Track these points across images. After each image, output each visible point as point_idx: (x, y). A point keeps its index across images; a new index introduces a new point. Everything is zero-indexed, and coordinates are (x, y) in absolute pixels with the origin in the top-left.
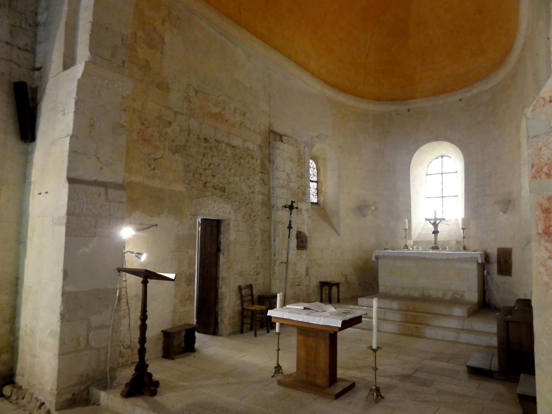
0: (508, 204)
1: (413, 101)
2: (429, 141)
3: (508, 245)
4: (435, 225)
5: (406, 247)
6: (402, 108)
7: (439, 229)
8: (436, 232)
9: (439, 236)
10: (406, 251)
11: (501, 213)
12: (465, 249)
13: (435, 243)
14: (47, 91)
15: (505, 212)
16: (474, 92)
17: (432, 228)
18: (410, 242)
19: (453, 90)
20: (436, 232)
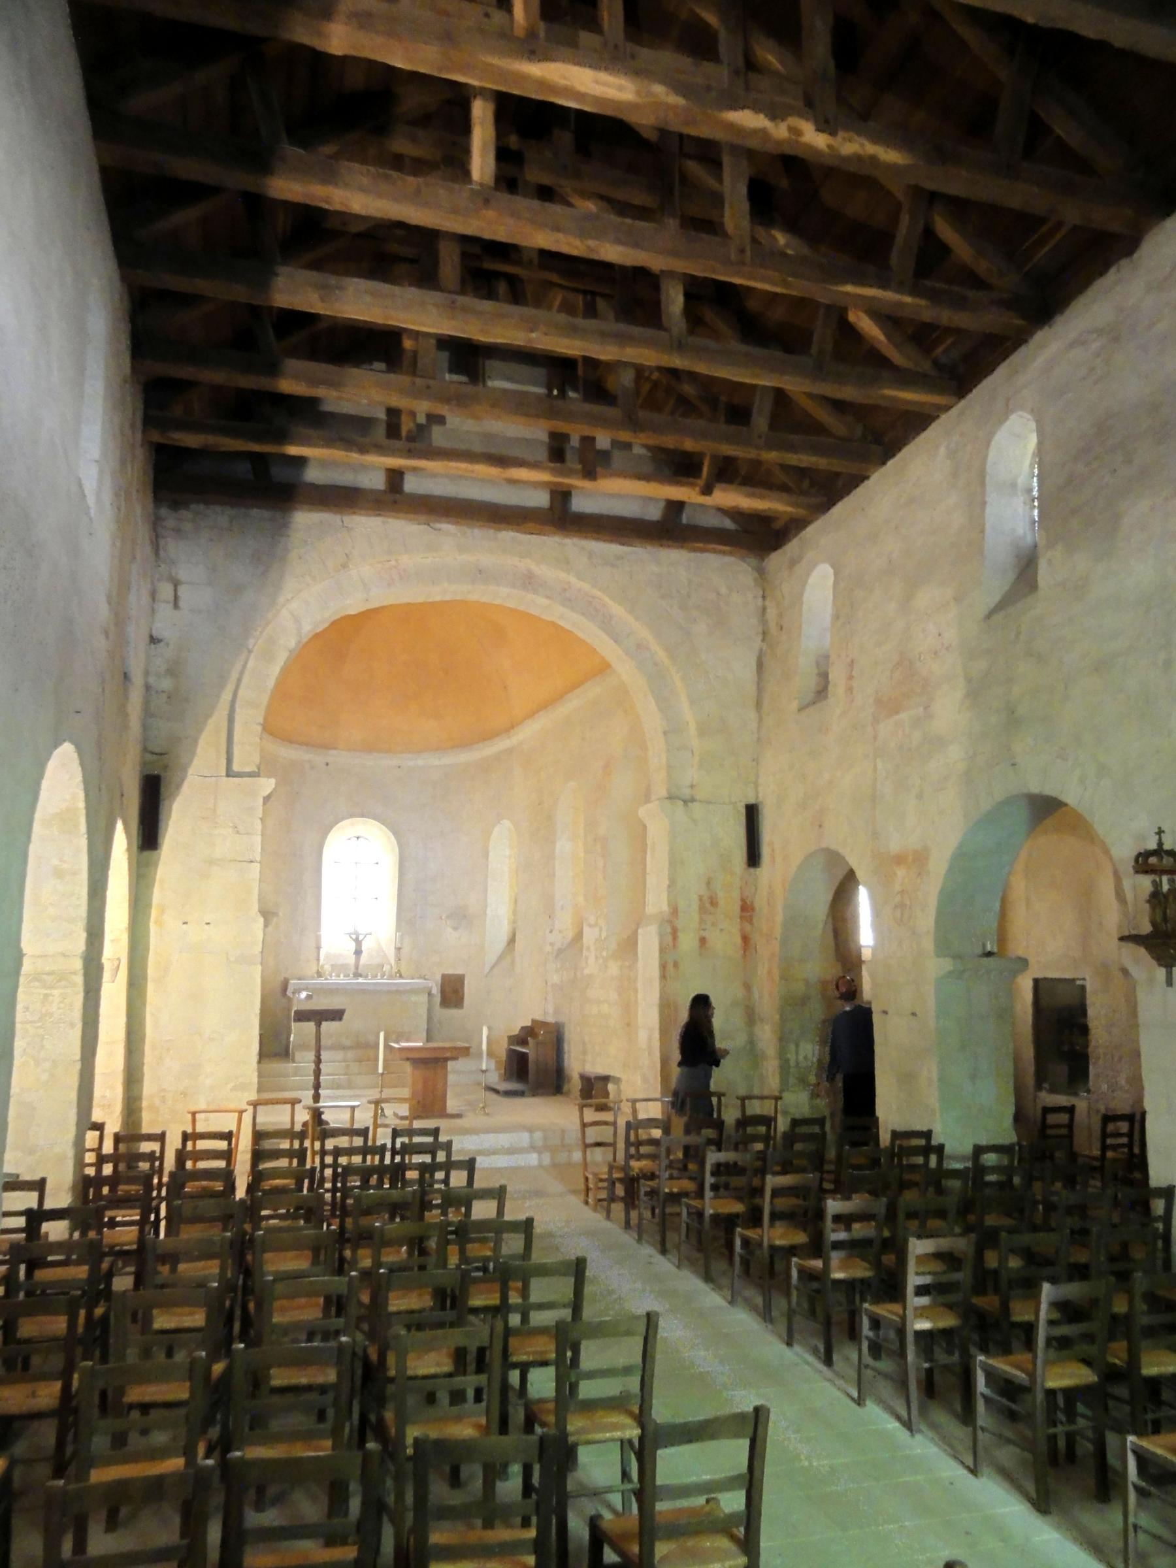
0: (461, 917)
1: (334, 752)
2: (352, 816)
3: (459, 971)
4: (358, 942)
5: (319, 975)
6: (318, 758)
7: (365, 947)
8: (358, 952)
9: (364, 959)
10: (321, 981)
11: (449, 930)
12: (401, 977)
13: (357, 967)
14: (186, 788)
15: (455, 929)
16: (420, 762)
17: (352, 946)
18: (327, 968)
19: (388, 751)
20: (358, 952)
